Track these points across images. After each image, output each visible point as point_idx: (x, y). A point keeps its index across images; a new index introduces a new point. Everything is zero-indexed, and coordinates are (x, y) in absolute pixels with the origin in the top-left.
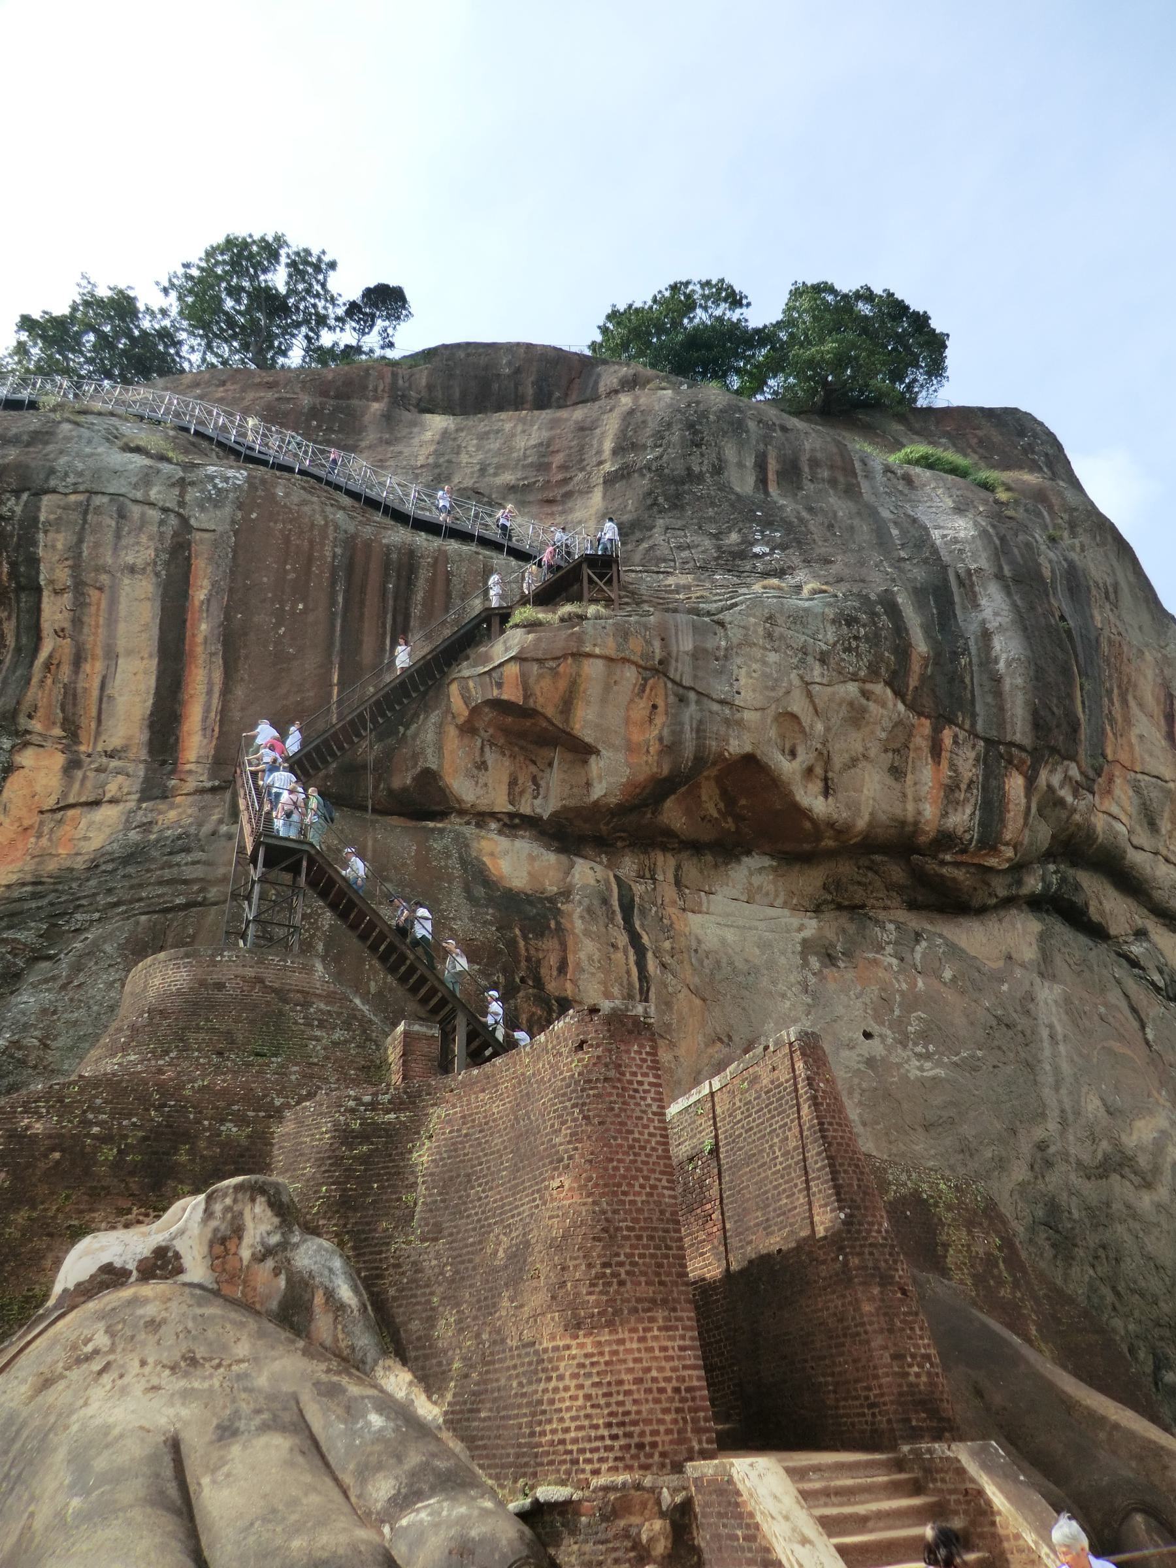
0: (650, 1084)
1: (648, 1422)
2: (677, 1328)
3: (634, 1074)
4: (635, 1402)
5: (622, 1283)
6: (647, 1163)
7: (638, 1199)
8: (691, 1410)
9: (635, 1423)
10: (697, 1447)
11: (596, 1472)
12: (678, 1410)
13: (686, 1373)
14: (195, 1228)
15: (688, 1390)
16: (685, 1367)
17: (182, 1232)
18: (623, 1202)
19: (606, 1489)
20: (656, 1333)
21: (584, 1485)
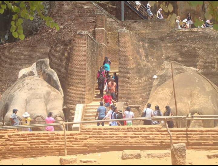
0: (84, 46)
1: (75, 99)
2: (81, 86)
3: (81, 45)
4: (74, 96)
5: (74, 80)
6: (81, 60)
7: (79, 67)
8: (82, 97)
9: (73, 99)
10: (82, 102)
11: (68, 105)
12: (80, 97)
13: (82, 92)
14: (35, 68)
15: (82, 95)
16: (82, 92)
17: (33, 69)
18: (76, 67)
19: (69, 107)
20: (78, 87)
21: (67, 106)
